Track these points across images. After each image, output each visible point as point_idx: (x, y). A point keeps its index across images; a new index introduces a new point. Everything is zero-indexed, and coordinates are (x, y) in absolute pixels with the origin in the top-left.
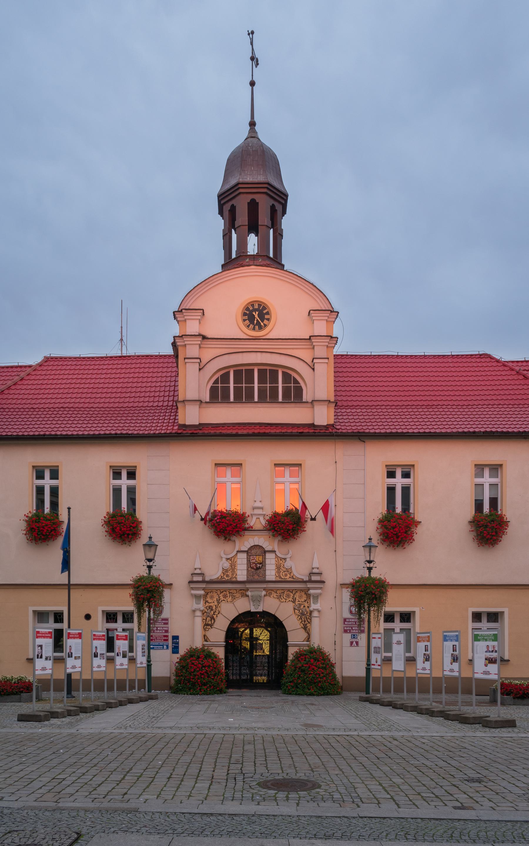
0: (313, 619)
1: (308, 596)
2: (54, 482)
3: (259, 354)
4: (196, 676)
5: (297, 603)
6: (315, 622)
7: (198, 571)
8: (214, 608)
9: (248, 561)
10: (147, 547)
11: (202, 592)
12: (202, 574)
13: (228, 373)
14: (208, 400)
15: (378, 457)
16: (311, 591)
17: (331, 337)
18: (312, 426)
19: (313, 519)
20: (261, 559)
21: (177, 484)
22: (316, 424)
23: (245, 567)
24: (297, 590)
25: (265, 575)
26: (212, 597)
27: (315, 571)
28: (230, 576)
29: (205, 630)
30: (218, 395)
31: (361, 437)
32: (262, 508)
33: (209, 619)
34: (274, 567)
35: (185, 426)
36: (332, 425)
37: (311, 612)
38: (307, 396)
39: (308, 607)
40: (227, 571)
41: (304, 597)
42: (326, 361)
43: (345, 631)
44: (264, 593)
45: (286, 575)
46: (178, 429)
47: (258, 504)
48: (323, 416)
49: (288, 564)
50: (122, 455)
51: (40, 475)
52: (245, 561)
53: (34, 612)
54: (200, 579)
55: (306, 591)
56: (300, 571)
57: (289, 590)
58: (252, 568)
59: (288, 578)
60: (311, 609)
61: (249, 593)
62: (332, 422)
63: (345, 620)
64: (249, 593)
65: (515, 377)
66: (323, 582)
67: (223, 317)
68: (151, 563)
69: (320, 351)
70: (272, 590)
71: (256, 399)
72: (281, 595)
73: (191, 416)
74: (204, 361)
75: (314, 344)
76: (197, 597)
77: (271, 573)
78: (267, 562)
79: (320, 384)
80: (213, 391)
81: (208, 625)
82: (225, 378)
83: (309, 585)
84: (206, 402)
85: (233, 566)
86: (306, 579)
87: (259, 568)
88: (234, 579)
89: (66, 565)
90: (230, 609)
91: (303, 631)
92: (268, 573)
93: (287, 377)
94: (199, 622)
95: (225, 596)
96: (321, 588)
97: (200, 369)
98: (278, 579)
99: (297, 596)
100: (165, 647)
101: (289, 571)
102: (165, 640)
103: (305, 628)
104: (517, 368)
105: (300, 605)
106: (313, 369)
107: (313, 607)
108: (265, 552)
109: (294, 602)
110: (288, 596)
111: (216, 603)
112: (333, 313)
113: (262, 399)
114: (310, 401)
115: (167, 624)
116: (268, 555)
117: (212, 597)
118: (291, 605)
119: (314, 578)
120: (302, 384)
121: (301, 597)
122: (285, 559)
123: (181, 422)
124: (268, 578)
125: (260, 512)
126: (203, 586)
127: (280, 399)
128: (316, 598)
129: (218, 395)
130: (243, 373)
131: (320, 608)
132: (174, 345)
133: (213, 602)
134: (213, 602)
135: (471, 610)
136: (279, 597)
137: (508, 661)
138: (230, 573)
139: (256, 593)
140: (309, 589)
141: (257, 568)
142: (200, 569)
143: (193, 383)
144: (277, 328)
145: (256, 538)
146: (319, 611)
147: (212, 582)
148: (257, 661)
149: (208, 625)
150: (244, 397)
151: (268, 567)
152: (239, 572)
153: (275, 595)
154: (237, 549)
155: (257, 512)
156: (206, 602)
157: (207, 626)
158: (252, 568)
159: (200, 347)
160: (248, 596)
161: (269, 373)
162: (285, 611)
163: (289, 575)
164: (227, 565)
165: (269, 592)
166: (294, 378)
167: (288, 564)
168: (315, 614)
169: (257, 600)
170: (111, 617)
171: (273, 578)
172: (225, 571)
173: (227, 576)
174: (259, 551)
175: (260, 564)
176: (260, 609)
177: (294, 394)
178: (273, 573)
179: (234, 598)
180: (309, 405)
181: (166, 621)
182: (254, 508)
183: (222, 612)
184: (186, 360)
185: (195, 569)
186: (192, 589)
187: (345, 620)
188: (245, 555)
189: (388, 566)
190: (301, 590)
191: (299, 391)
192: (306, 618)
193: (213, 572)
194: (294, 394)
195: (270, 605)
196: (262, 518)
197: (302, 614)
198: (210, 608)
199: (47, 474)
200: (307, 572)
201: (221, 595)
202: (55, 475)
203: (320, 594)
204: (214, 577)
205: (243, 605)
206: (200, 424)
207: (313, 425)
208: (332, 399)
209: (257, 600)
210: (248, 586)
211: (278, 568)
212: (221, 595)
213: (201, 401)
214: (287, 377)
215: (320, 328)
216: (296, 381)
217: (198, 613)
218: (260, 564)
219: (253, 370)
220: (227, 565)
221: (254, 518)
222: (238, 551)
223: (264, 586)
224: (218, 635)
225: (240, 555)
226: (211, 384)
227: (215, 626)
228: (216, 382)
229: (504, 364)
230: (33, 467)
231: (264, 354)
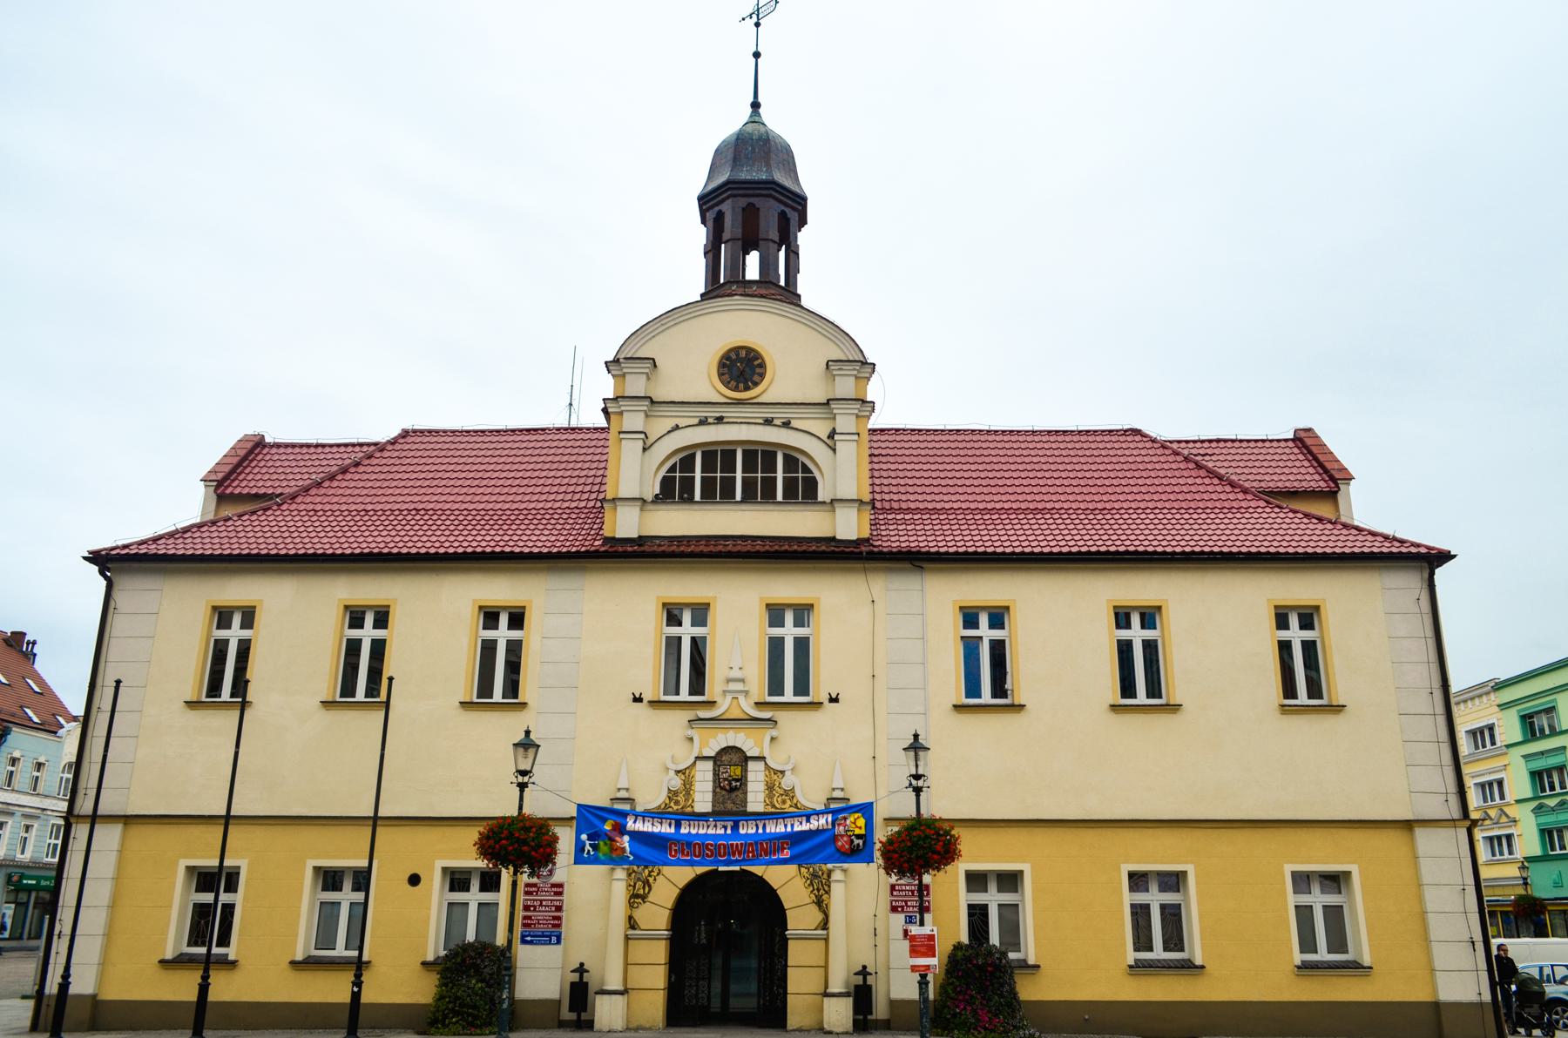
9: (716, 774)
13: (693, 456)
15: (946, 594)
17: (864, 401)
20: (738, 771)
22: (838, 537)
23: (710, 786)
25: (745, 802)
27: (837, 794)
29: (631, 906)
30: (673, 490)
32: (742, 680)
33: (639, 884)
34: (762, 787)
35: (613, 539)
36: (868, 540)
38: (823, 494)
40: (676, 793)
43: (894, 909)
45: (784, 802)
47: (736, 674)
48: (849, 526)
49: (787, 782)
52: (710, 776)
58: (723, 788)
59: (787, 807)
62: (866, 534)
69: (845, 423)
71: (738, 497)
73: (625, 524)
78: (751, 776)
80: (667, 483)
82: (687, 463)
87: (736, 788)
91: (814, 908)
92: (750, 797)
93: (791, 463)
97: (644, 449)
100: (554, 939)
101: (790, 793)
103: (819, 903)
106: (834, 450)
108: (746, 759)
113: (749, 496)
115: (560, 894)
116: (751, 765)
120: (817, 474)
122: (783, 772)
123: (607, 533)
124: (751, 808)
127: (780, 497)
129: (673, 490)
130: (718, 457)
132: (605, 411)
135: (1126, 868)
137: (1203, 967)
138: (681, 798)
145: (731, 734)
150: (718, 492)
151: (750, 787)
152: (697, 797)
158: (723, 788)
161: (760, 456)
164: (677, 783)
170: (458, 880)
171: (760, 808)
172: (672, 794)
173: (677, 803)
174: (735, 757)
177: (803, 489)
178: (761, 797)
180: (828, 508)
181: (558, 888)
182: (729, 681)
188: (709, 765)
191: (811, 487)
194: (803, 489)
207: (833, 539)
208: (867, 497)
211: (770, 788)
213: (644, 501)
214: (791, 463)
215: (845, 387)
216: (806, 469)
220: (677, 783)
222: (697, 758)
225: (700, 765)
226: (662, 472)
227: (650, 898)
228: (672, 469)
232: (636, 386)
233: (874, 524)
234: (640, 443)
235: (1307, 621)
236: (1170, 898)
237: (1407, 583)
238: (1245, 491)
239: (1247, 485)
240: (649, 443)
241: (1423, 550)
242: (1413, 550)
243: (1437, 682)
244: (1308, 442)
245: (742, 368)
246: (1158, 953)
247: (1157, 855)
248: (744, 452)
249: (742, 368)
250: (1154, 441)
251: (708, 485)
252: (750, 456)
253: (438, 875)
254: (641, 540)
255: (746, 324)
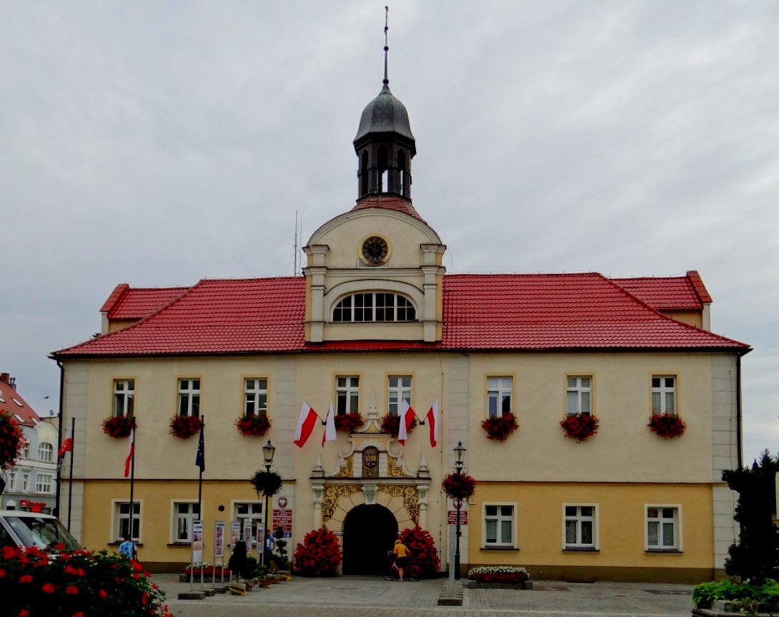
0: (421, 511)
1: (417, 491)
2: (196, 392)
3: (376, 281)
4: (317, 560)
5: (407, 497)
6: (422, 514)
7: (318, 469)
8: (333, 501)
9: (364, 460)
10: (267, 450)
11: (322, 487)
12: (323, 472)
13: (350, 298)
14: (332, 320)
16: (419, 487)
17: (440, 267)
18: (422, 342)
19: (422, 423)
21: (300, 391)
23: (361, 465)
24: (407, 486)
25: (378, 472)
26: (331, 492)
27: (423, 469)
28: (347, 473)
29: (324, 520)
30: (341, 315)
31: (465, 352)
32: (376, 414)
33: (328, 511)
34: (386, 465)
37: (419, 505)
39: (417, 501)
40: (344, 469)
41: (414, 492)
42: (435, 287)
43: (450, 523)
44: (377, 488)
45: (397, 472)
46: (304, 346)
47: (373, 410)
48: (431, 334)
49: (399, 463)
50: (254, 369)
51: (184, 386)
52: (361, 460)
53: (176, 504)
54: (320, 475)
55: (415, 487)
56: (410, 470)
57: (399, 486)
58: (367, 466)
59: (398, 475)
60: (419, 503)
61: (363, 488)
62: (440, 339)
63: (449, 513)
64: (363, 488)
65: (618, 295)
66: (429, 479)
67: (349, 253)
68: (269, 464)
70: (385, 486)
72: (392, 490)
73: (316, 335)
74: (328, 289)
75: (425, 272)
76: (318, 492)
77: (383, 471)
79: (429, 305)
81: (326, 516)
83: (417, 482)
84: (330, 323)
85: (350, 465)
86: (415, 476)
87: (373, 466)
88: (351, 476)
89: (200, 461)
90: (347, 503)
93: (402, 300)
94: (318, 513)
95: (343, 491)
96: (428, 484)
97: (325, 295)
98: (390, 476)
99: (407, 491)
100: (288, 535)
101: (399, 469)
102: (288, 529)
104: (621, 286)
105: (410, 499)
106: (424, 293)
107: (421, 501)
109: (404, 496)
110: (399, 491)
111: (334, 497)
112: (441, 247)
114: (420, 321)
115: (290, 515)
116: (381, 455)
117: (331, 492)
118: (402, 499)
119: (422, 475)
121: (410, 492)
122: (396, 459)
123: (307, 339)
124: (381, 475)
125: (375, 417)
126: (323, 481)
128: (424, 492)
129: (341, 315)
131: (426, 502)
133: (332, 496)
134: (332, 496)
136: (391, 492)
138: (347, 471)
139: (370, 488)
140: (417, 485)
141: (371, 468)
142: (321, 467)
143: (319, 307)
144: (395, 257)
145: (371, 440)
146: (426, 505)
147: (330, 478)
148: (371, 546)
149: (326, 516)
152: (354, 470)
153: (386, 489)
154: (353, 450)
155: (372, 417)
156: (326, 495)
157: (327, 516)
158: (367, 466)
159: (325, 276)
160: (362, 491)
161: (385, 298)
162: (395, 504)
163: (399, 473)
164: (344, 463)
165: (381, 487)
166: (408, 302)
167: (399, 463)
168: (422, 507)
169: (371, 494)
171: (385, 475)
172: (343, 469)
173: (345, 473)
174: (373, 452)
175: (374, 462)
176: (374, 503)
177: (408, 314)
178: (386, 470)
179: (350, 492)
182: (370, 414)
183: (339, 504)
184: (313, 288)
185: (317, 467)
186: (314, 484)
187: (449, 513)
188: (361, 455)
189: (484, 461)
190: (411, 486)
191: (412, 312)
192: (414, 511)
193: (333, 470)
194: (408, 314)
195: (382, 499)
196: (376, 422)
197: (412, 507)
198: (330, 501)
199: (191, 385)
200: (416, 471)
201: (339, 490)
202: (197, 385)
203: (427, 489)
204: (333, 474)
205: (358, 499)
206: (324, 341)
209: (371, 494)
210: (362, 482)
211: (390, 466)
212: (339, 490)
213: (325, 323)
216: (409, 304)
217: (318, 506)
218: (374, 462)
219: (372, 295)
220: (344, 463)
221: (369, 423)
222: (354, 452)
223: (377, 482)
224: (336, 526)
226: (334, 307)
227: (333, 517)
228: (339, 305)
229: (610, 282)
230: (179, 379)
231: (381, 281)
232: (319, 260)
233: (445, 332)
234: (322, 292)
235: (670, 383)
236: (586, 519)
237: (726, 363)
238: (650, 309)
239: (652, 306)
240: (327, 291)
241: (736, 345)
242: (731, 345)
243: (735, 415)
244: (693, 279)
245: (375, 249)
246: (579, 544)
247: (580, 498)
248: (377, 295)
249: (375, 249)
250: (605, 280)
251: (358, 313)
252: (380, 297)
253: (232, 506)
254: (325, 343)
255: (381, 223)
